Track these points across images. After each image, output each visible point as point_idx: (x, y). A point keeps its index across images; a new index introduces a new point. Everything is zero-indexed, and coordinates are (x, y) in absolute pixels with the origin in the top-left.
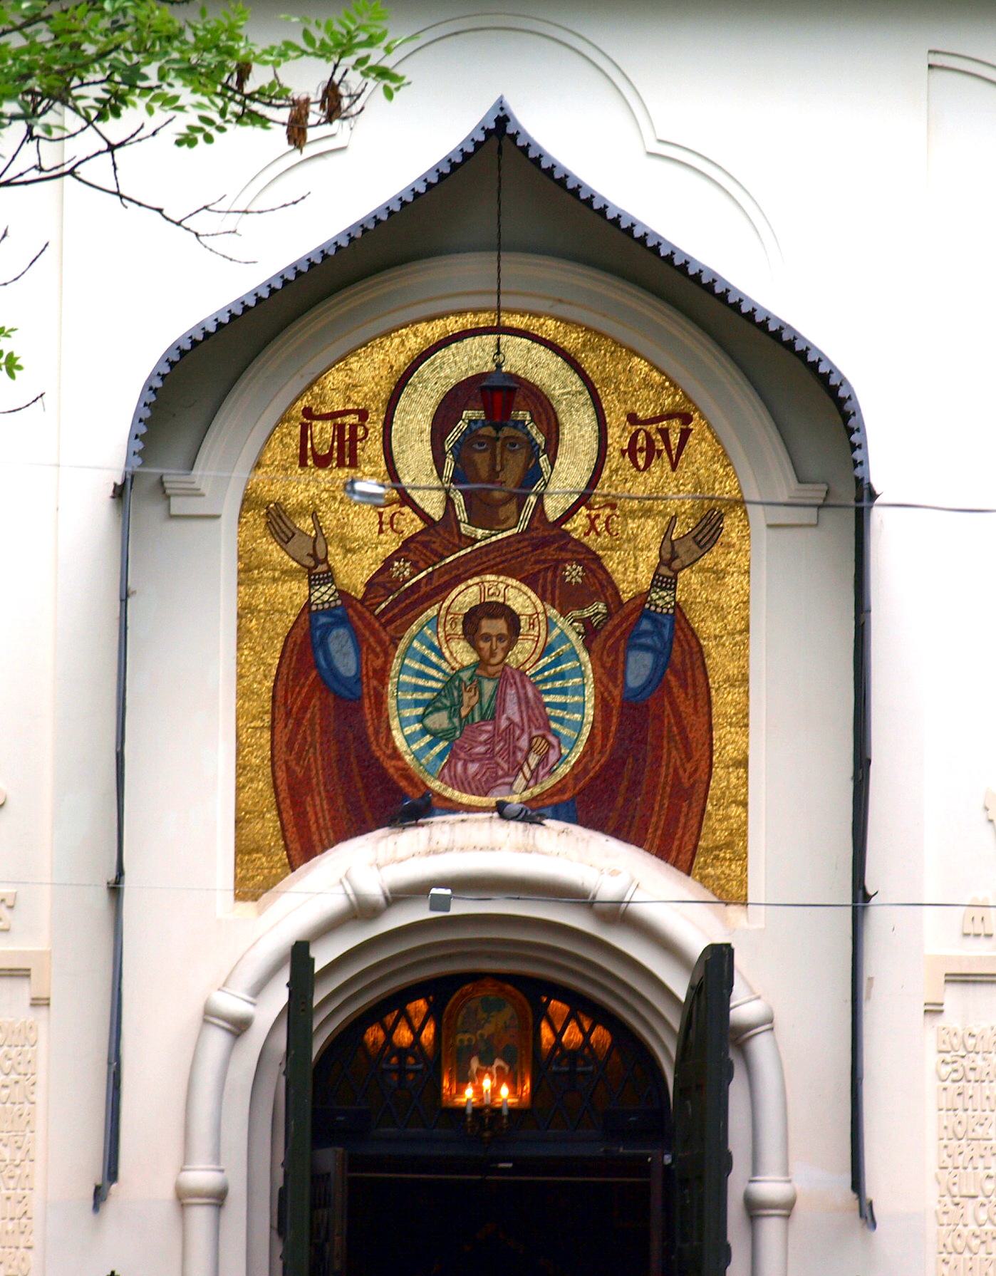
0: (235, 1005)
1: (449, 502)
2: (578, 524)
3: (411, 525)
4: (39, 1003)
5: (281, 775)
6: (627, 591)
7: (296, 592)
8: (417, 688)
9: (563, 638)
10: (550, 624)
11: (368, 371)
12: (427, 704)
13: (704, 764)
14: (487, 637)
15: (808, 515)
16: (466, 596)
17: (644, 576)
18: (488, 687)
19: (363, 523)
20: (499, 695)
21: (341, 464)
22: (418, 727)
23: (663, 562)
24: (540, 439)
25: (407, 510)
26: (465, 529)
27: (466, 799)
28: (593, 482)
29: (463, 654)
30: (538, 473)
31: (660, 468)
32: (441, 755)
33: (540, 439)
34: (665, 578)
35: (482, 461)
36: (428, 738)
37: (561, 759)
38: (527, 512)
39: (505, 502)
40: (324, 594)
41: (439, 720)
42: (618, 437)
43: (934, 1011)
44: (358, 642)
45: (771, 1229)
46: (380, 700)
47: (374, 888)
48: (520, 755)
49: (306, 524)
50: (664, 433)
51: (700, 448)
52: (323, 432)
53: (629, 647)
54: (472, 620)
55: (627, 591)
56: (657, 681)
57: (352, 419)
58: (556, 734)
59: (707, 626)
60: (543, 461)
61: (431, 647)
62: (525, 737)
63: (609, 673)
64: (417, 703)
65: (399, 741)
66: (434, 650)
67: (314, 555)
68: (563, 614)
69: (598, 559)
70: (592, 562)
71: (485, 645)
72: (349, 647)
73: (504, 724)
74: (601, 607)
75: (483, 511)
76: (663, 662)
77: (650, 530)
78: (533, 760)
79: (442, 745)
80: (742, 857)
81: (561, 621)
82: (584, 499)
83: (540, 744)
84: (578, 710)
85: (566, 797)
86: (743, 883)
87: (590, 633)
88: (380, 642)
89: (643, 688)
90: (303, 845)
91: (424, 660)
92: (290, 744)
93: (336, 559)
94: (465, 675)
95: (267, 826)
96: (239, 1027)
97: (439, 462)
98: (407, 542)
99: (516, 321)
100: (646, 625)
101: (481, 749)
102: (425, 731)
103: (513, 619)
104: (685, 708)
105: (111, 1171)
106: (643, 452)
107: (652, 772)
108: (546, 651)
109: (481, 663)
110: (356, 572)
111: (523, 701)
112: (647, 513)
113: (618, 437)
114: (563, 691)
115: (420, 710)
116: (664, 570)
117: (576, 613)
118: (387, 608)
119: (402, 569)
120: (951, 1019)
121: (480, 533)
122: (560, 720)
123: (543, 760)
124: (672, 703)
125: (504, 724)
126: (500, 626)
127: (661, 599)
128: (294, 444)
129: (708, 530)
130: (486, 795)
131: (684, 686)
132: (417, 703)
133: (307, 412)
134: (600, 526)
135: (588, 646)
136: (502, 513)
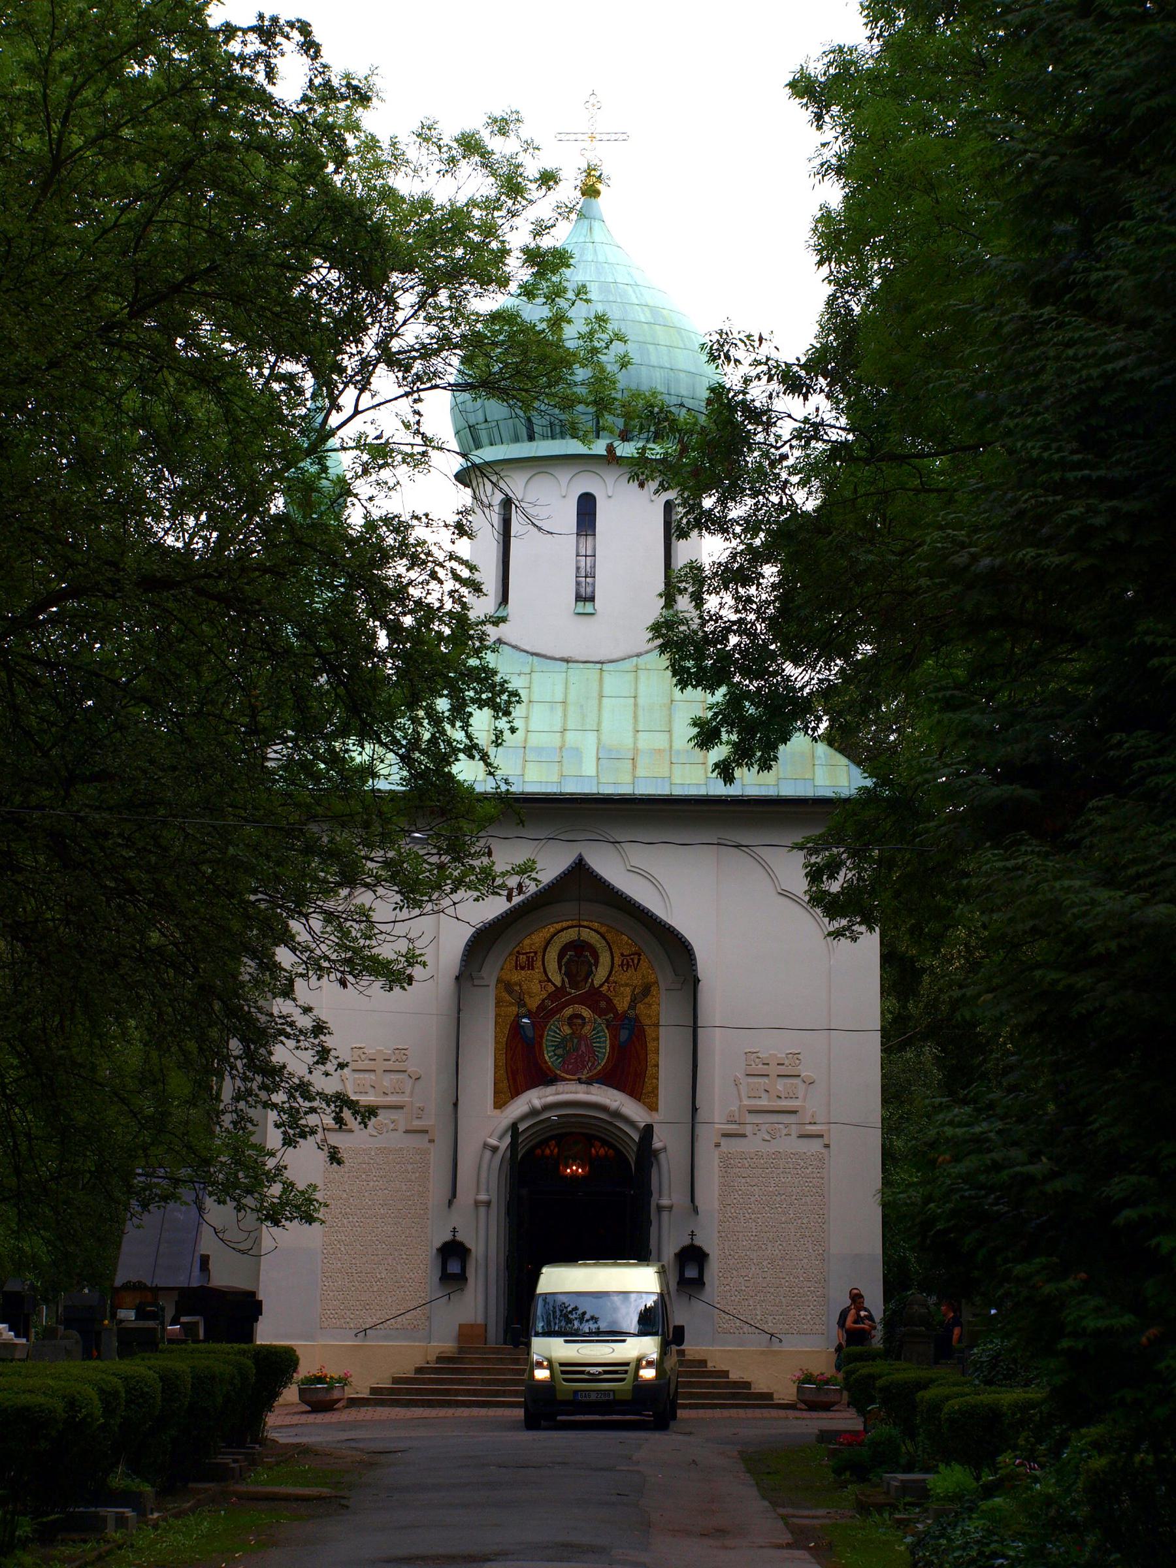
0: (493, 1142)
1: (563, 981)
3: (551, 989)
4: (431, 1141)
6: (620, 1009)
7: (514, 1010)
11: (538, 939)
16: (568, 1011)
17: (626, 1005)
19: (535, 987)
28: (609, 976)
29: (567, 1030)
31: (631, 971)
34: (633, 1004)
38: (588, 985)
41: (560, 1051)
42: (617, 961)
45: (665, 1215)
47: (537, 1103)
49: (517, 988)
51: (644, 964)
52: (523, 958)
59: (646, 1021)
63: (614, 1037)
66: (558, 1030)
70: (609, 1001)
75: (574, 984)
77: (628, 990)
80: (657, 1095)
81: (599, 1021)
82: (607, 981)
84: (604, 1048)
86: (657, 1104)
90: (516, 1092)
93: (527, 999)
95: (504, 1084)
96: (495, 1149)
99: (585, 923)
103: (583, 1018)
105: (454, 1195)
106: (626, 966)
107: (629, 1069)
109: (573, 1033)
110: (533, 1004)
111: (587, 1045)
112: (627, 985)
113: (617, 961)
118: (542, 1016)
120: (723, 1148)
129: (646, 990)
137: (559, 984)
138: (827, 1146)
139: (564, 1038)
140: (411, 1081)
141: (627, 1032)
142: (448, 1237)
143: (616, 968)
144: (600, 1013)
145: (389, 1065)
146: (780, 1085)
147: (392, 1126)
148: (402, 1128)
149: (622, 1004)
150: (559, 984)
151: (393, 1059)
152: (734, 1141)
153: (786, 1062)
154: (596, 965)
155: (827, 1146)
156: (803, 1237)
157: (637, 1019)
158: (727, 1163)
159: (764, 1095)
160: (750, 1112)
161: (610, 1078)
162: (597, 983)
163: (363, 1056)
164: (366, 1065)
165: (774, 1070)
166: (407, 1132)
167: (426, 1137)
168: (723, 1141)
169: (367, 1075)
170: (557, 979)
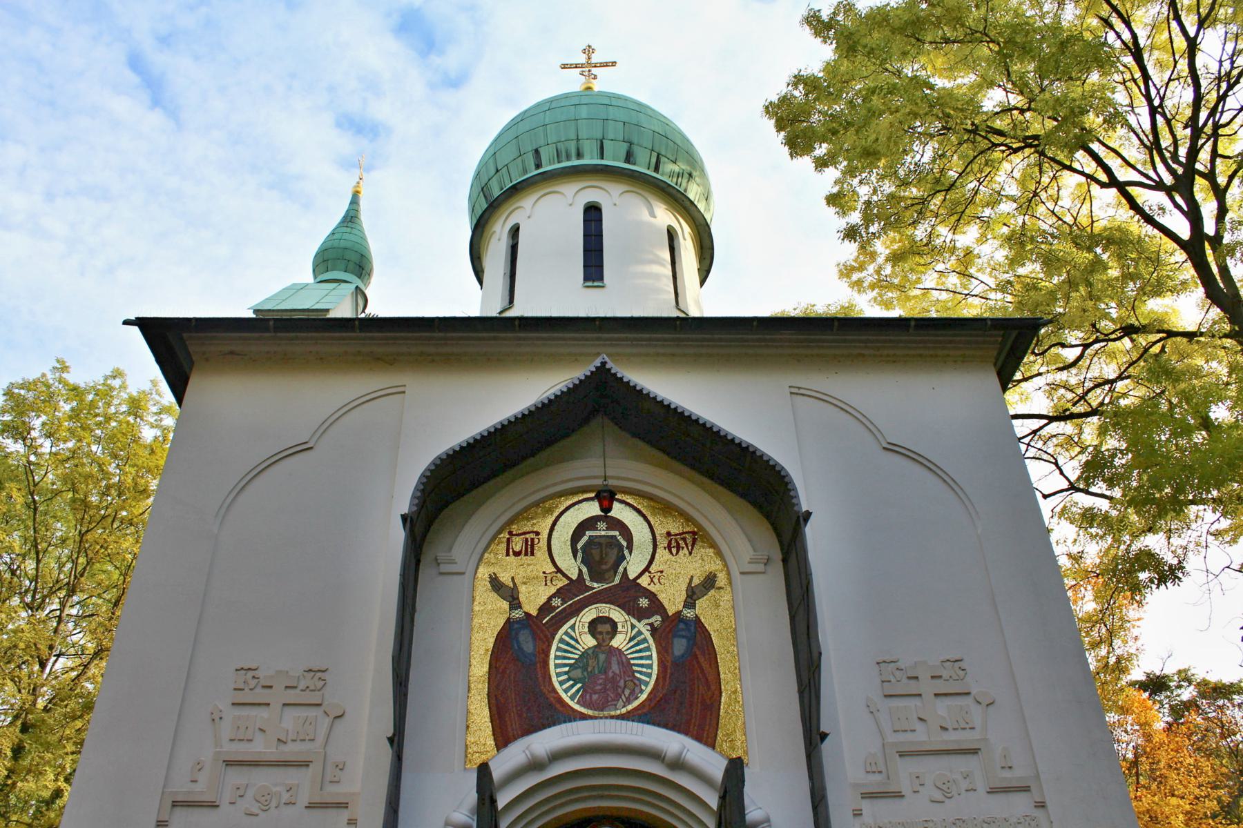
1: (580, 571)
2: (644, 581)
3: (563, 582)
5: (493, 701)
9: (640, 633)
10: (633, 627)
13: (717, 692)
14: (601, 633)
15: (761, 567)
16: (589, 614)
18: (602, 657)
20: (608, 662)
21: (526, 554)
24: (625, 544)
25: (559, 575)
27: (590, 712)
29: (589, 642)
30: (624, 558)
32: (578, 691)
33: (625, 544)
34: (690, 602)
35: (596, 553)
37: (642, 691)
39: (608, 570)
40: (517, 614)
44: (535, 637)
50: (684, 539)
52: (518, 544)
53: (675, 636)
54: (593, 625)
57: (532, 536)
58: (639, 679)
60: (626, 552)
61: (572, 638)
64: (565, 665)
65: (557, 685)
66: (578, 634)
67: (512, 596)
69: (654, 595)
70: (652, 597)
71: (600, 637)
72: (530, 639)
73: (611, 674)
76: (692, 641)
78: (627, 692)
79: (579, 685)
82: (646, 569)
83: (630, 684)
84: (649, 671)
87: (654, 630)
88: (546, 636)
91: (568, 644)
92: (497, 687)
93: (522, 598)
94: (590, 652)
97: (575, 557)
100: (682, 626)
101: (599, 687)
103: (614, 625)
104: (705, 665)
107: (689, 694)
108: (631, 639)
111: (621, 663)
114: (641, 658)
115: (567, 669)
117: (647, 621)
119: (556, 602)
120: (867, 818)
121: (595, 585)
122: (640, 673)
123: (633, 692)
124: (698, 662)
125: (611, 674)
126: (607, 627)
127: (689, 613)
128: (504, 546)
131: (703, 654)
132: (565, 665)
134: (656, 580)
137: (574, 577)
138: (1041, 805)
139: (585, 655)
140: (327, 721)
141: (684, 641)
143: (660, 551)
144: (640, 614)
145: (292, 697)
146: (943, 708)
147: (286, 797)
148: (304, 799)
149: (672, 599)
150: (574, 577)
151: (302, 685)
153: (945, 674)
155: (1041, 805)
159: (919, 726)
160: (902, 755)
162: (632, 576)
163: (253, 683)
164: (260, 695)
168: (866, 805)
170: (572, 566)
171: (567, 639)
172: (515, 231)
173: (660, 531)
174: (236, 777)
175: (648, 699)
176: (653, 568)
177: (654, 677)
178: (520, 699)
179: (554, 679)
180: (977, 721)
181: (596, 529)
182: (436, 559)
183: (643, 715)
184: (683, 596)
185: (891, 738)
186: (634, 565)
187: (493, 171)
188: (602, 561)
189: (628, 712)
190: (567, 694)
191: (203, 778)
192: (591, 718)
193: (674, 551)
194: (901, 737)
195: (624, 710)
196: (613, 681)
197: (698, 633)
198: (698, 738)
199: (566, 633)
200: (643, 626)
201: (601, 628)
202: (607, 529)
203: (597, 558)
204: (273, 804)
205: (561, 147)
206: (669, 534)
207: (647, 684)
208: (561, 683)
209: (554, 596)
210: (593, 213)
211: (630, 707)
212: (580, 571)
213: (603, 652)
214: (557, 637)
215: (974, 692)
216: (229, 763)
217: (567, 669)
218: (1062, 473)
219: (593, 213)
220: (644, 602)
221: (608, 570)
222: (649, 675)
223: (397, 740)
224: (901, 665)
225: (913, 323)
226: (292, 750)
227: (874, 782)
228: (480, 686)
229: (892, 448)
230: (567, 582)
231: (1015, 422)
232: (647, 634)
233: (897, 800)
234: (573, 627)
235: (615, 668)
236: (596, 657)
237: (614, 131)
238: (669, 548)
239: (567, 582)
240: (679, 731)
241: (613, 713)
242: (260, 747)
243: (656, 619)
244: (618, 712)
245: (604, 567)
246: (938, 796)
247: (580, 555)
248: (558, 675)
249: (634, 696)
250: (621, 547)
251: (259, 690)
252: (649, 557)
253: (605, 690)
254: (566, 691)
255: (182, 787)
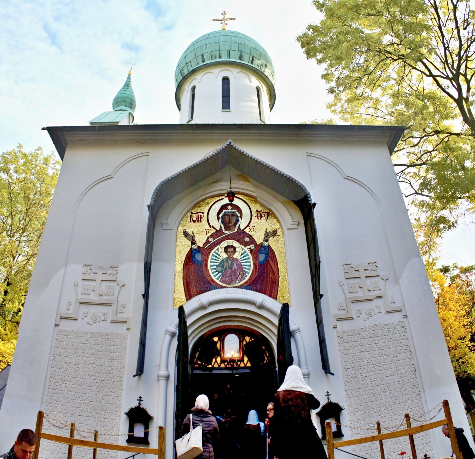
1: (221, 226)
2: (247, 230)
3: (213, 231)
4: (128, 329)
5: (185, 281)
6: (258, 243)
8: (214, 262)
9: (245, 252)
10: (243, 249)
12: (217, 265)
13: (277, 276)
14: (229, 252)
16: (225, 244)
18: (230, 262)
20: (232, 264)
22: (215, 270)
23: (265, 237)
24: (239, 215)
26: (224, 231)
29: (224, 256)
32: (220, 276)
33: (239, 215)
34: (266, 239)
35: (227, 219)
36: (217, 273)
37: (246, 276)
39: (232, 226)
41: (220, 269)
42: (255, 214)
43: (335, 327)
46: (206, 265)
48: (237, 276)
53: (259, 253)
54: (226, 249)
55: (258, 243)
56: (266, 260)
58: (245, 271)
60: (240, 218)
61: (217, 254)
62: (238, 272)
63: (255, 258)
64: (215, 265)
66: (219, 252)
68: (245, 247)
69: (251, 236)
70: (250, 237)
73: (233, 269)
74: (253, 246)
75: (227, 228)
76: (267, 255)
78: (240, 277)
79: (220, 274)
82: (248, 225)
83: (242, 273)
85: (248, 284)
87: (251, 251)
88: (206, 253)
89: (263, 261)
91: (216, 257)
94: (225, 260)
97: (218, 220)
98: (212, 235)
100: (263, 249)
102: (216, 271)
103: (235, 249)
104: (272, 265)
108: (242, 254)
109: (228, 257)
114: (246, 262)
115: (215, 267)
116: (266, 238)
119: (211, 239)
120: (339, 329)
121: (227, 232)
122: (246, 268)
124: (270, 264)
125: (233, 269)
126: (232, 250)
127: (265, 244)
130: (230, 284)
132: (215, 265)
133: (192, 213)
135: (251, 253)
136: (232, 228)
137: (218, 229)
140: (119, 287)
141: (264, 255)
142: (135, 404)
144: (246, 244)
147: (102, 318)
148: (109, 319)
149: (259, 238)
150: (218, 229)
151: (109, 273)
152: (344, 323)
153: (370, 269)
154: (241, 217)
156: (404, 383)
157: (269, 247)
158: (342, 338)
159: (359, 290)
160: (353, 302)
161: (252, 285)
162: (242, 228)
163: (90, 271)
165: (362, 274)
166: (112, 322)
167: (125, 326)
168: (338, 324)
169: (90, 283)
170: (217, 224)
171: (215, 254)
172: (194, 89)
173: (254, 210)
174: (84, 308)
175: (249, 279)
176: (251, 225)
177: (251, 270)
178: (196, 280)
179: (210, 271)
180: (382, 288)
181: (227, 209)
182: (161, 223)
183: (247, 286)
184: (263, 236)
185: (349, 295)
186: (243, 224)
187: (185, 64)
188: (229, 222)
189: (241, 285)
190: (215, 277)
191: (71, 308)
192: (225, 287)
193: (259, 218)
194: (353, 295)
195: (239, 284)
196: (235, 272)
197: (269, 252)
198: (270, 296)
199: (215, 252)
200: (247, 249)
201: (229, 250)
202: (232, 209)
203: (228, 221)
204: (98, 320)
205: (213, 53)
206: (257, 211)
207: (248, 273)
208: (213, 273)
209: (210, 237)
210: (226, 81)
211: (241, 283)
212: (221, 226)
213: (230, 260)
214: (211, 254)
215: (380, 275)
216: (81, 303)
217: (215, 267)
218: (412, 187)
219: (226, 81)
220: (247, 239)
221: (232, 226)
222: (249, 269)
223: (146, 296)
224: (352, 265)
225: (356, 128)
226: (105, 299)
227: (342, 314)
228: (180, 274)
229: (347, 178)
230: (215, 231)
231: (395, 167)
232: (249, 253)
233: (351, 321)
234: (218, 250)
235: (235, 266)
236: (228, 262)
237: (235, 47)
238: (257, 216)
239: (215, 231)
240: (262, 293)
241: (234, 285)
242: (93, 297)
243: (252, 246)
244: (237, 285)
245: (230, 225)
246: (366, 317)
247: (220, 220)
248: (212, 269)
249: (243, 278)
250: (237, 217)
251: (92, 274)
252: (249, 221)
253: (231, 276)
254: (215, 276)
255: (64, 312)
